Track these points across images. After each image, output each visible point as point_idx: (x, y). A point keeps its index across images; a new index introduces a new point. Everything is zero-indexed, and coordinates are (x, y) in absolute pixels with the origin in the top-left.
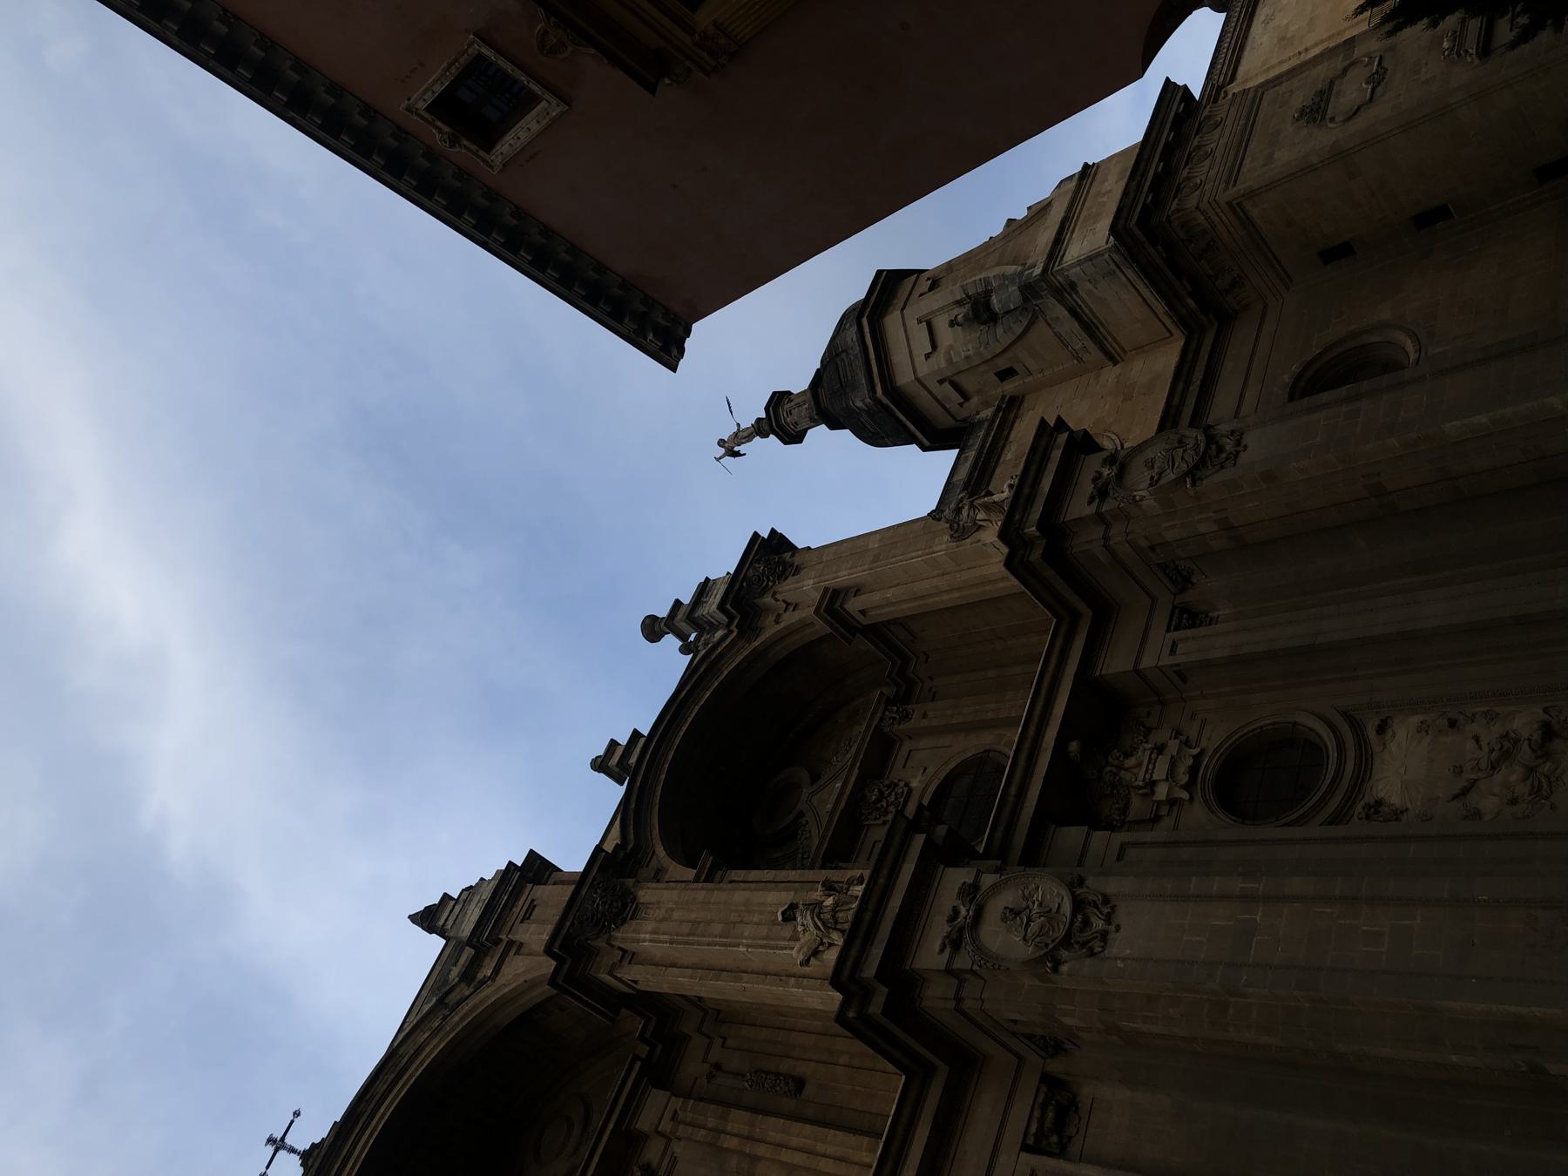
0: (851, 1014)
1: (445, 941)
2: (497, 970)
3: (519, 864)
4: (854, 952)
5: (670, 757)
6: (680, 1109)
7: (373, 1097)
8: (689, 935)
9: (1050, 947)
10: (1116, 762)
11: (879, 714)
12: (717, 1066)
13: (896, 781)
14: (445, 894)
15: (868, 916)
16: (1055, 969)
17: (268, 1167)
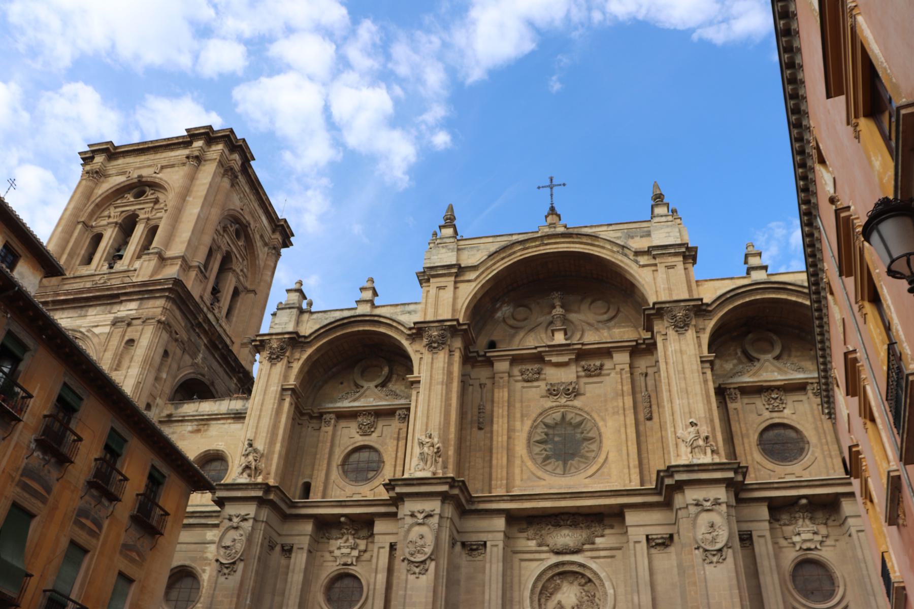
0: (662, 474)
1: (650, 219)
2: (644, 266)
3: (689, 246)
4: (681, 469)
5: (758, 297)
6: (626, 371)
7: (580, 238)
8: (678, 371)
9: (703, 545)
10: (805, 516)
11: (814, 381)
12: (646, 375)
13: (785, 402)
14: (668, 204)
15: (696, 468)
16: (696, 549)
17: (543, 187)
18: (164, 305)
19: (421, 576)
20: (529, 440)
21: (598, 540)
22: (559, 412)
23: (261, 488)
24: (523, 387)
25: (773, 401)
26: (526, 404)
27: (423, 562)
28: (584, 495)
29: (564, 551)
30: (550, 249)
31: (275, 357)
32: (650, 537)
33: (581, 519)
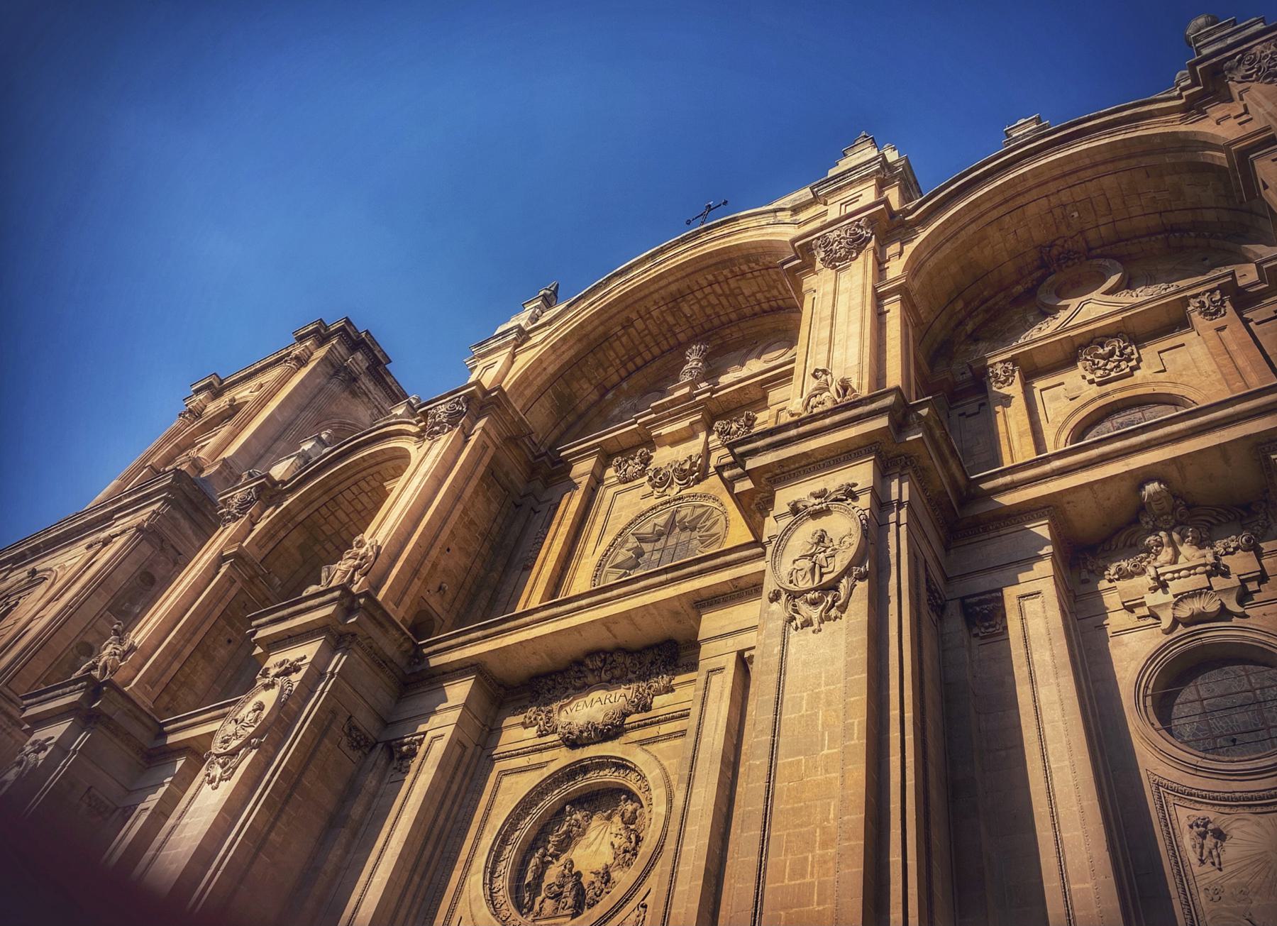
0: (726, 474)
15: (793, 432)
18: (159, 508)
19: (222, 783)
20: (600, 566)
21: (658, 701)
22: (668, 511)
23: (81, 688)
24: (617, 493)
25: (1102, 362)
26: (616, 514)
27: (233, 753)
28: (615, 592)
29: (585, 734)
30: (664, 267)
31: (230, 517)
32: (747, 655)
33: (628, 661)
